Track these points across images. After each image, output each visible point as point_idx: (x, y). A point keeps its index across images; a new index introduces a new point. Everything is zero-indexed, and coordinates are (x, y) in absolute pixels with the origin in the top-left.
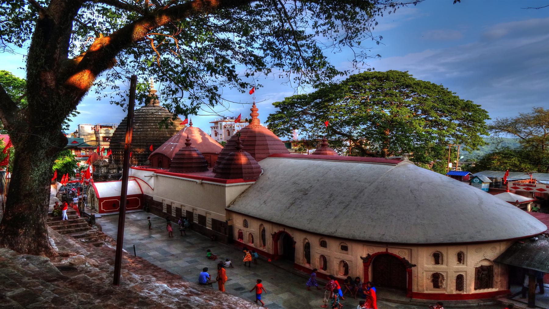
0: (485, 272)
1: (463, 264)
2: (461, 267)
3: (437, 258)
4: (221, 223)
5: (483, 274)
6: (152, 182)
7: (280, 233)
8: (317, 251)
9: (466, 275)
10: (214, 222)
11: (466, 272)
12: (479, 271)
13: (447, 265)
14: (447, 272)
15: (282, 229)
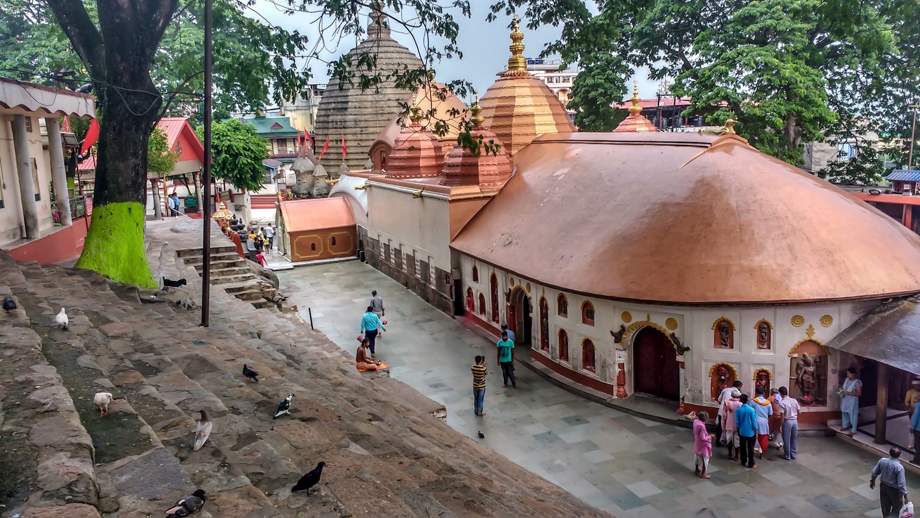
0: (811, 369)
1: (769, 348)
2: (765, 353)
3: (724, 334)
4: (447, 276)
5: (805, 372)
6: (363, 198)
7: (519, 290)
8: (556, 321)
9: (774, 370)
10: (439, 272)
11: (773, 365)
12: (798, 365)
13: (740, 350)
14: (740, 364)
15: (517, 284)
